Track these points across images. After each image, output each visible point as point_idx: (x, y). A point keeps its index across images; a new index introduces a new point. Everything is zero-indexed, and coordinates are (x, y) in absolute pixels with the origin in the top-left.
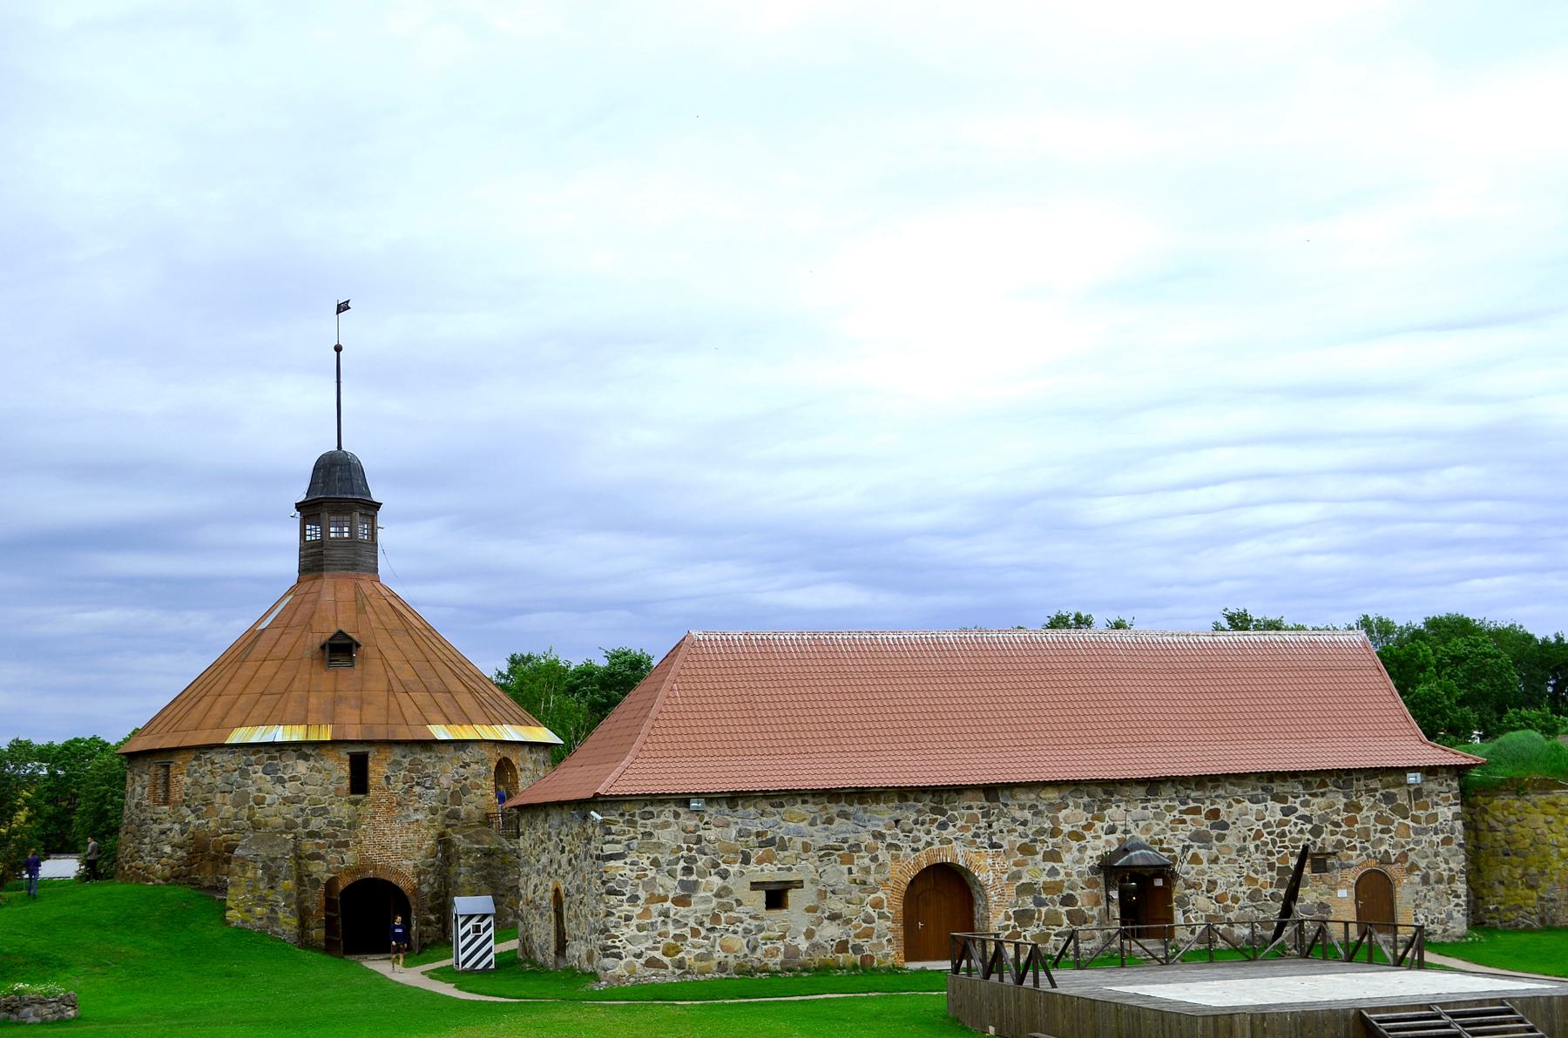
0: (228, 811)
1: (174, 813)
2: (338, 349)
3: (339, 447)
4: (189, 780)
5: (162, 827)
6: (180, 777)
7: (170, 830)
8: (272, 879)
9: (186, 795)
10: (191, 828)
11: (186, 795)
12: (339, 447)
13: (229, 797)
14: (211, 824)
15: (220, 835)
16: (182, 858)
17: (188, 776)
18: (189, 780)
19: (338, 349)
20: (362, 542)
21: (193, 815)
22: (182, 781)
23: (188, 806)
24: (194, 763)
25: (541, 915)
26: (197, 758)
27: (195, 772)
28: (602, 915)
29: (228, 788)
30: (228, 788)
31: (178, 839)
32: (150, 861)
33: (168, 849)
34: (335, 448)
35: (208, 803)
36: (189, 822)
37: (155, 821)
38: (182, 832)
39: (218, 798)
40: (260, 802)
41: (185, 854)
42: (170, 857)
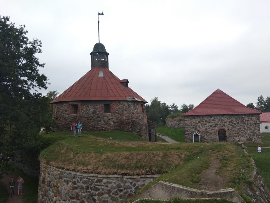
0: (127, 115)
1: (113, 115)
2: (99, 22)
3: (99, 41)
4: (117, 108)
5: (109, 118)
6: (115, 107)
7: (112, 119)
8: (146, 129)
9: (117, 111)
10: (119, 118)
11: (117, 111)
12: (99, 41)
13: (127, 112)
14: (124, 118)
15: (126, 120)
16: (117, 125)
17: (117, 107)
18: (117, 108)
19: (99, 22)
20: (106, 61)
21: (119, 116)
22: (115, 107)
23: (118, 113)
24: (118, 104)
25: (211, 134)
26: (118, 103)
27: (119, 106)
28: (257, 132)
29: (126, 110)
30: (126, 110)
31: (115, 121)
32: (105, 126)
33: (113, 123)
34: (98, 42)
35: (123, 113)
36: (118, 117)
37: (106, 117)
38: (117, 119)
39: (125, 112)
40: (133, 113)
41: (118, 124)
42: (114, 125)
